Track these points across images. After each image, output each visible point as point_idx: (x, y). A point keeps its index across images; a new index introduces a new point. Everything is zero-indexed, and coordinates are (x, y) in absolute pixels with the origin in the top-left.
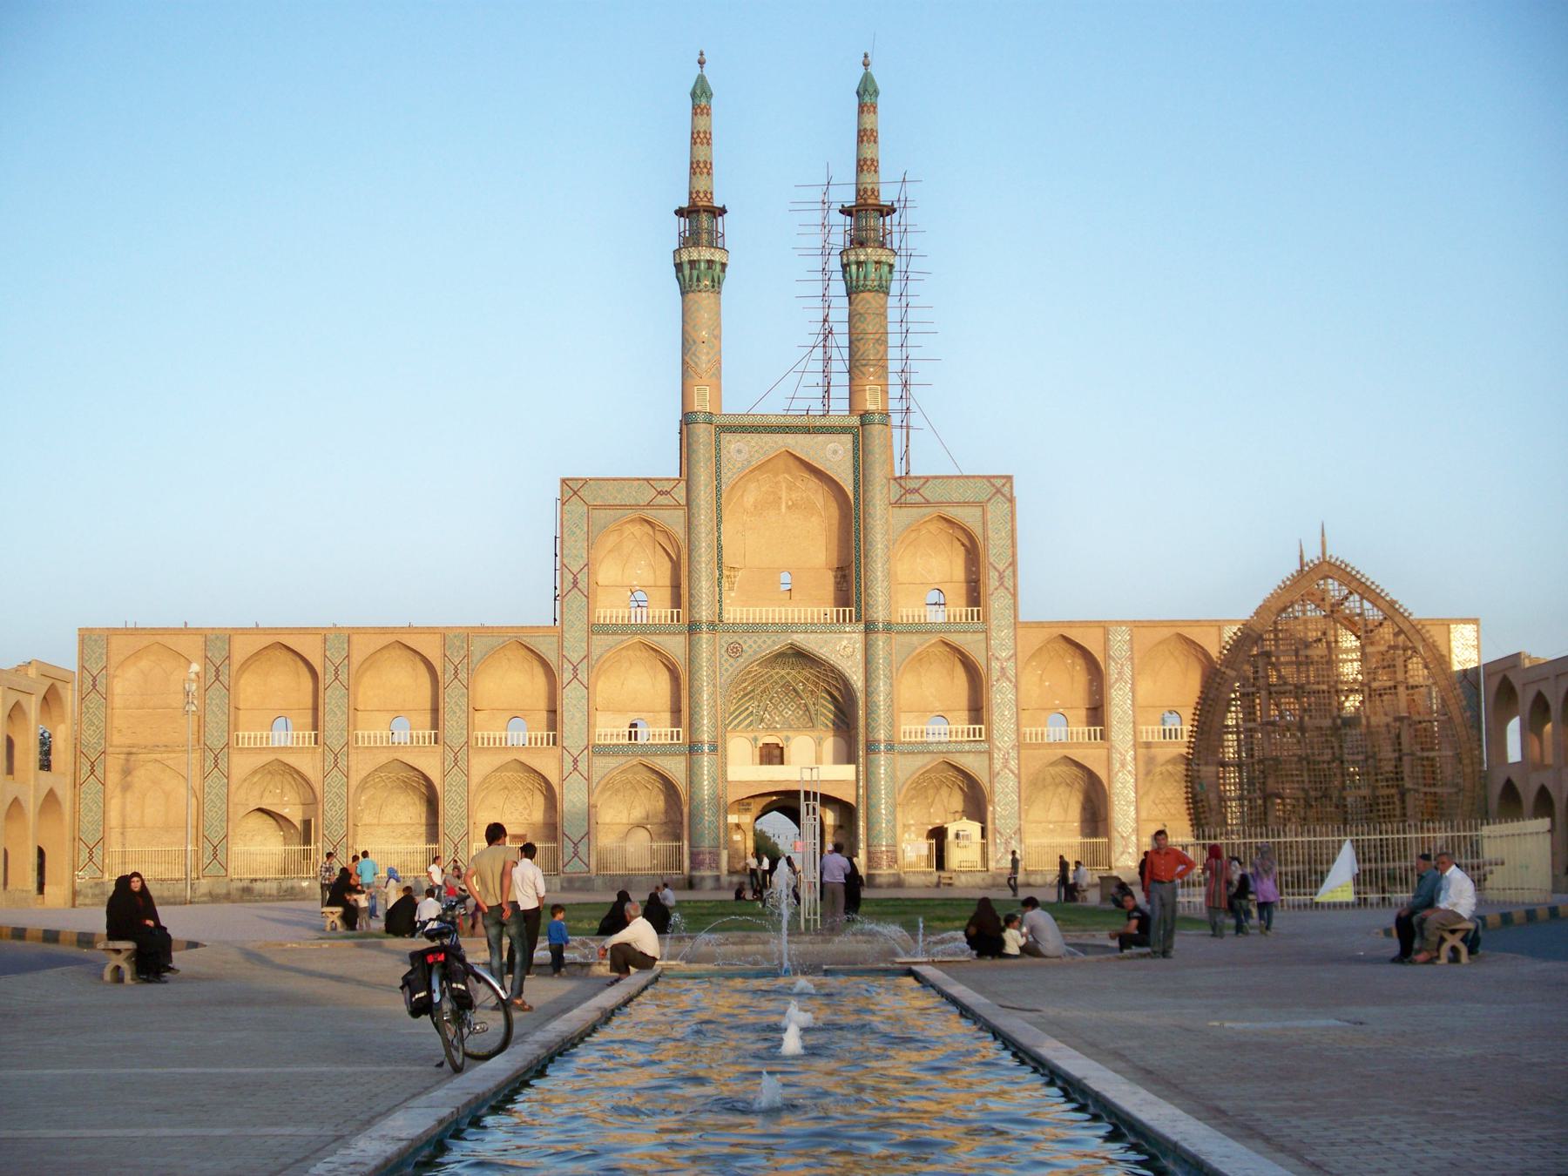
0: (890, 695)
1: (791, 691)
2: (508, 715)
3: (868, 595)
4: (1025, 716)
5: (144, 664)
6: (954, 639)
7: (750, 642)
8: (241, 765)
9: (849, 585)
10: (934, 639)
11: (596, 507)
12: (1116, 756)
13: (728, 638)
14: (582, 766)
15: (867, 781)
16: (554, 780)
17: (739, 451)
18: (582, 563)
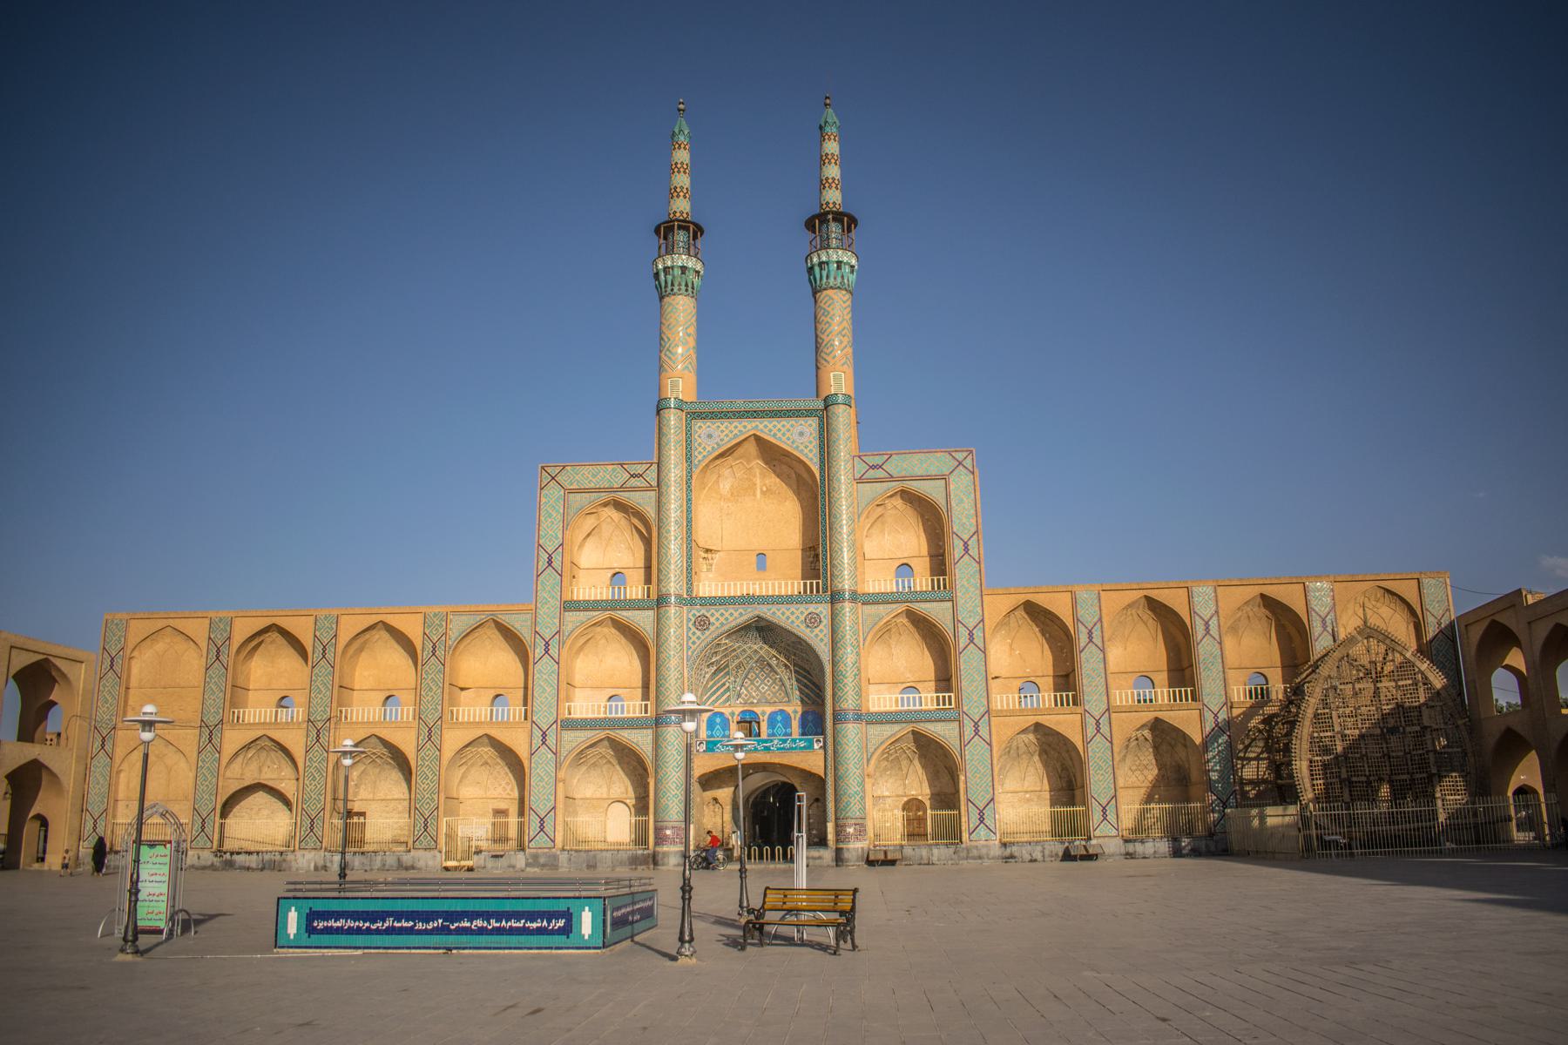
0: (857, 663)
1: (764, 664)
2: (493, 693)
3: (833, 566)
4: (993, 684)
5: (160, 646)
6: (923, 608)
7: (717, 615)
8: (232, 739)
9: (816, 559)
10: (902, 608)
11: (572, 491)
12: (1091, 722)
13: (698, 611)
14: (551, 740)
15: (835, 756)
16: (523, 752)
17: (710, 436)
18: (557, 543)
